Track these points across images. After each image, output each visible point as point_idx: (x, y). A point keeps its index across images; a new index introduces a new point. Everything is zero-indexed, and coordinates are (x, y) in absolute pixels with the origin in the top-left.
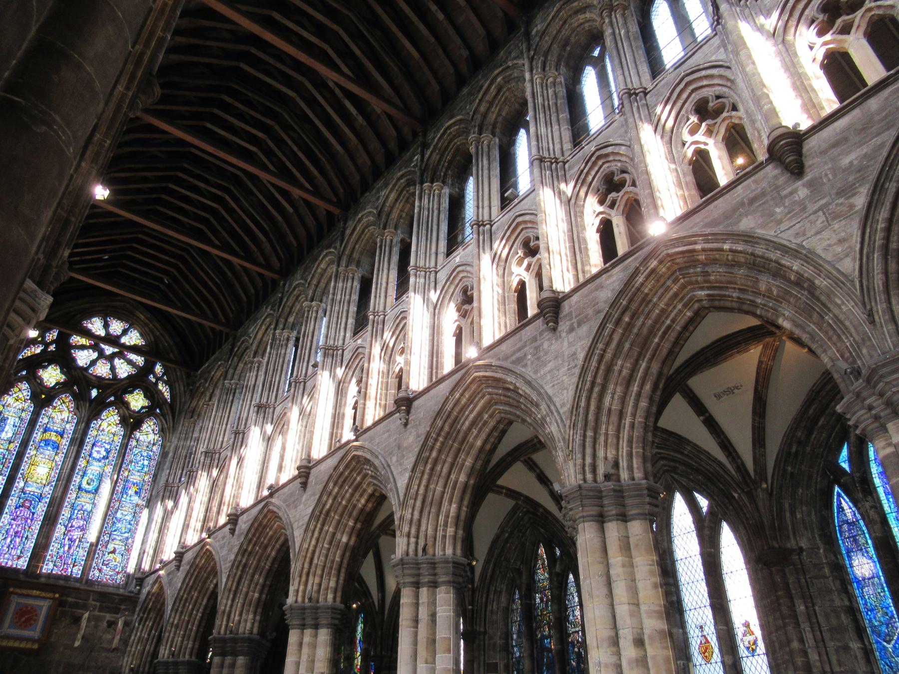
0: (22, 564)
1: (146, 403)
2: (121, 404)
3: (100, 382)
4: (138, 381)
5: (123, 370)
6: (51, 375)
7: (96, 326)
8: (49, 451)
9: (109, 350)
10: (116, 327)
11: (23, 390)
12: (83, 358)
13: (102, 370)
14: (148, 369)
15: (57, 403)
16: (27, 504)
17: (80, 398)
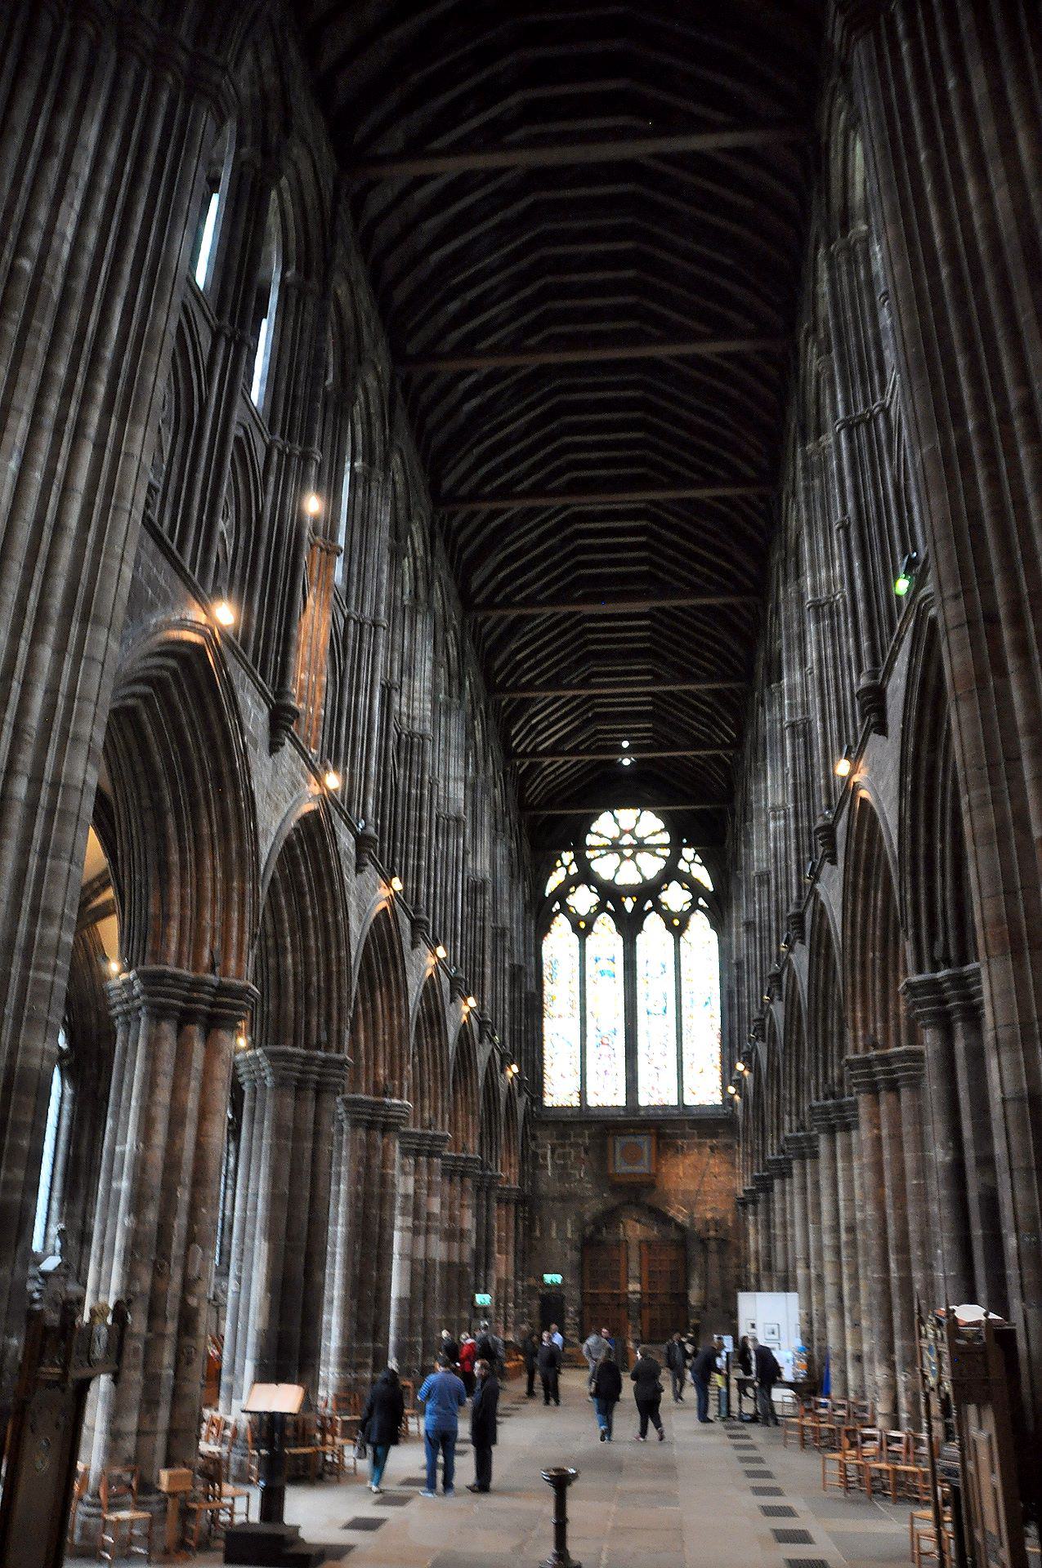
0: (621, 1101)
1: (689, 896)
2: (658, 907)
3: (630, 891)
4: (671, 873)
5: (651, 866)
6: (583, 899)
7: (606, 825)
8: (606, 981)
9: (627, 840)
10: (627, 816)
11: (561, 924)
12: (605, 867)
13: (628, 876)
14: (676, 856)
15: (596, 927)
16: (605, 1041)
17: (619, 916)
